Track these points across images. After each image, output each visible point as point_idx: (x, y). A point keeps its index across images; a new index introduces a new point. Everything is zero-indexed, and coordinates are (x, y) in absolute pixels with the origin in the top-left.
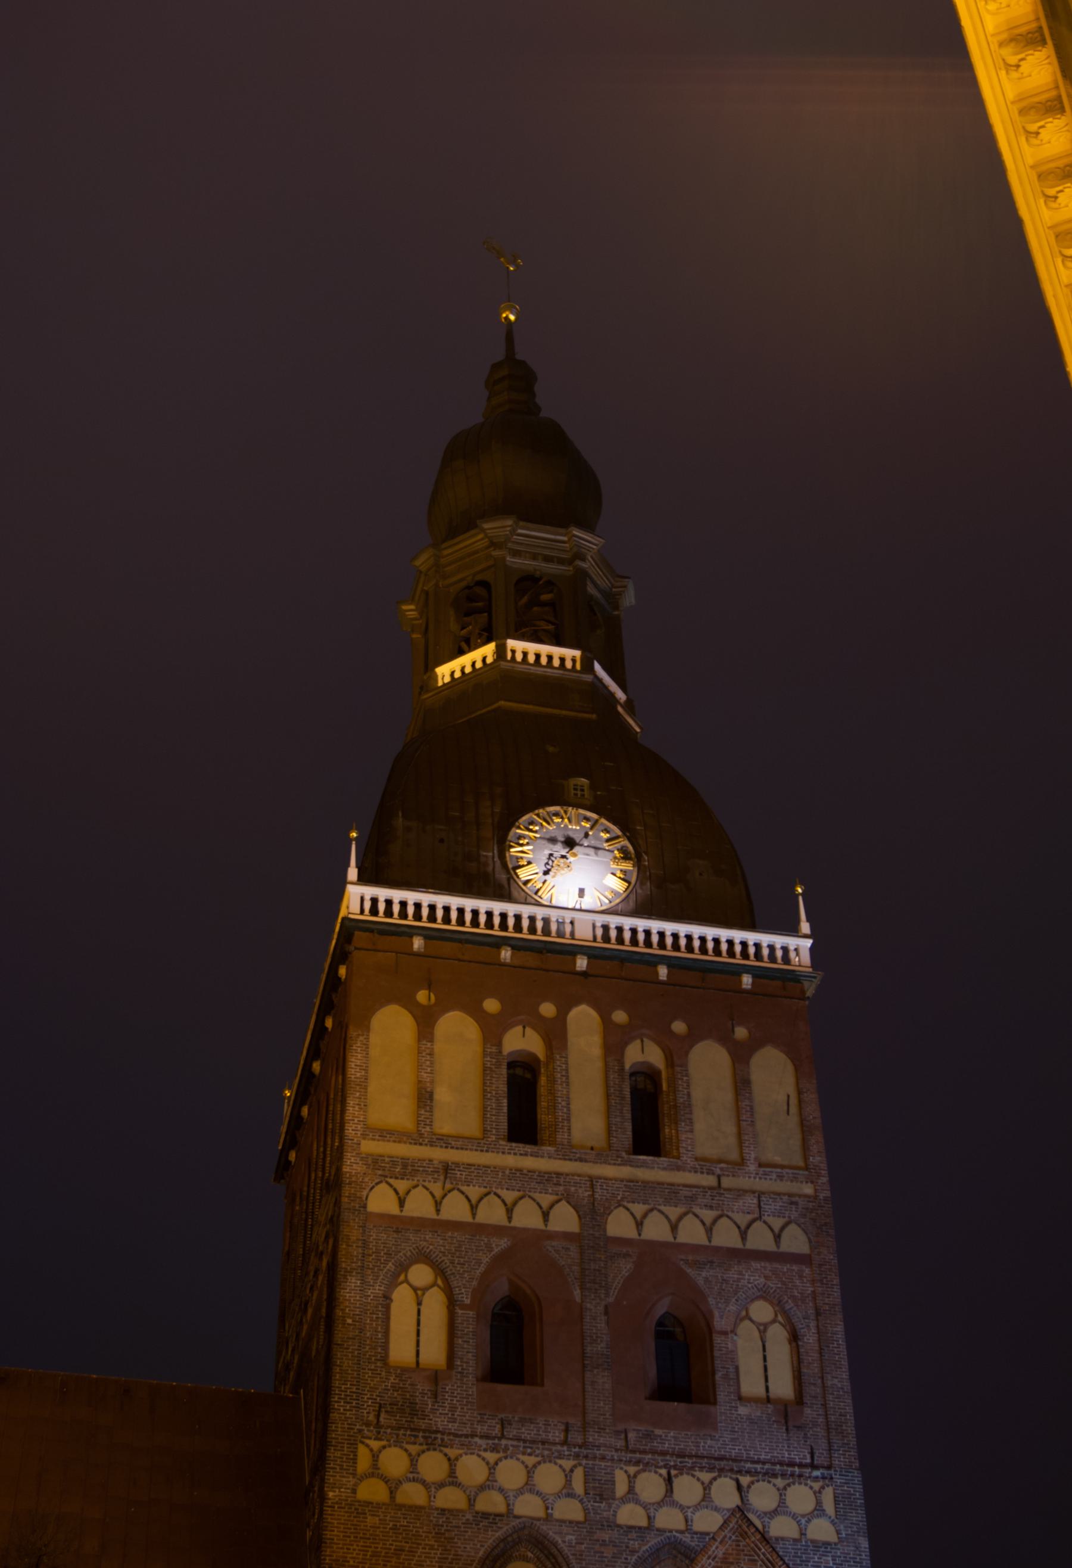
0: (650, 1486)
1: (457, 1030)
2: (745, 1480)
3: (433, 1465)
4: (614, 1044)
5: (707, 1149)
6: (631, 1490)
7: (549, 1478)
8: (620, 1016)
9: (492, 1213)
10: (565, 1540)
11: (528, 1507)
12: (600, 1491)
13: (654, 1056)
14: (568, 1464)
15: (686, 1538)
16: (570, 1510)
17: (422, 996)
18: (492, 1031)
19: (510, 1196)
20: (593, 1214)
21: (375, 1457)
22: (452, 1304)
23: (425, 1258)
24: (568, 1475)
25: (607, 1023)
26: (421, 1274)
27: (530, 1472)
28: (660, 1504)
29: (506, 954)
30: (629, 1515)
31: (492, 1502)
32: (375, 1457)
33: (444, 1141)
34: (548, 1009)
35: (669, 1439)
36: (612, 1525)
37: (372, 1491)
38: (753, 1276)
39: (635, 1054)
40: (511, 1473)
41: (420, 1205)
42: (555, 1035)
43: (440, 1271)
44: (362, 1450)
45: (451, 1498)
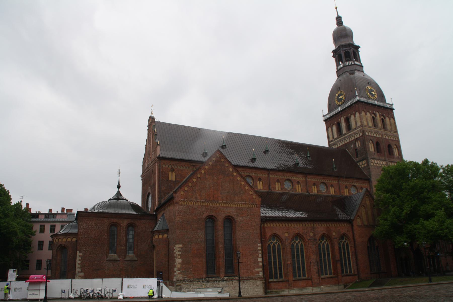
0: (391, 164)
1: (368, 114)
7: (384, 163)
9: (375, 135)
12: (387, 164)
13: (382, 117)
18: (371, 114)
20: (382, 136)
22: (374, 145)
23: (371, 140)
25: (379, 114)
26: (371, 142)
31: (380, 165)
33: (369, 127)
37: (372, 164)
40: (381, 162)
41: (370, 134)
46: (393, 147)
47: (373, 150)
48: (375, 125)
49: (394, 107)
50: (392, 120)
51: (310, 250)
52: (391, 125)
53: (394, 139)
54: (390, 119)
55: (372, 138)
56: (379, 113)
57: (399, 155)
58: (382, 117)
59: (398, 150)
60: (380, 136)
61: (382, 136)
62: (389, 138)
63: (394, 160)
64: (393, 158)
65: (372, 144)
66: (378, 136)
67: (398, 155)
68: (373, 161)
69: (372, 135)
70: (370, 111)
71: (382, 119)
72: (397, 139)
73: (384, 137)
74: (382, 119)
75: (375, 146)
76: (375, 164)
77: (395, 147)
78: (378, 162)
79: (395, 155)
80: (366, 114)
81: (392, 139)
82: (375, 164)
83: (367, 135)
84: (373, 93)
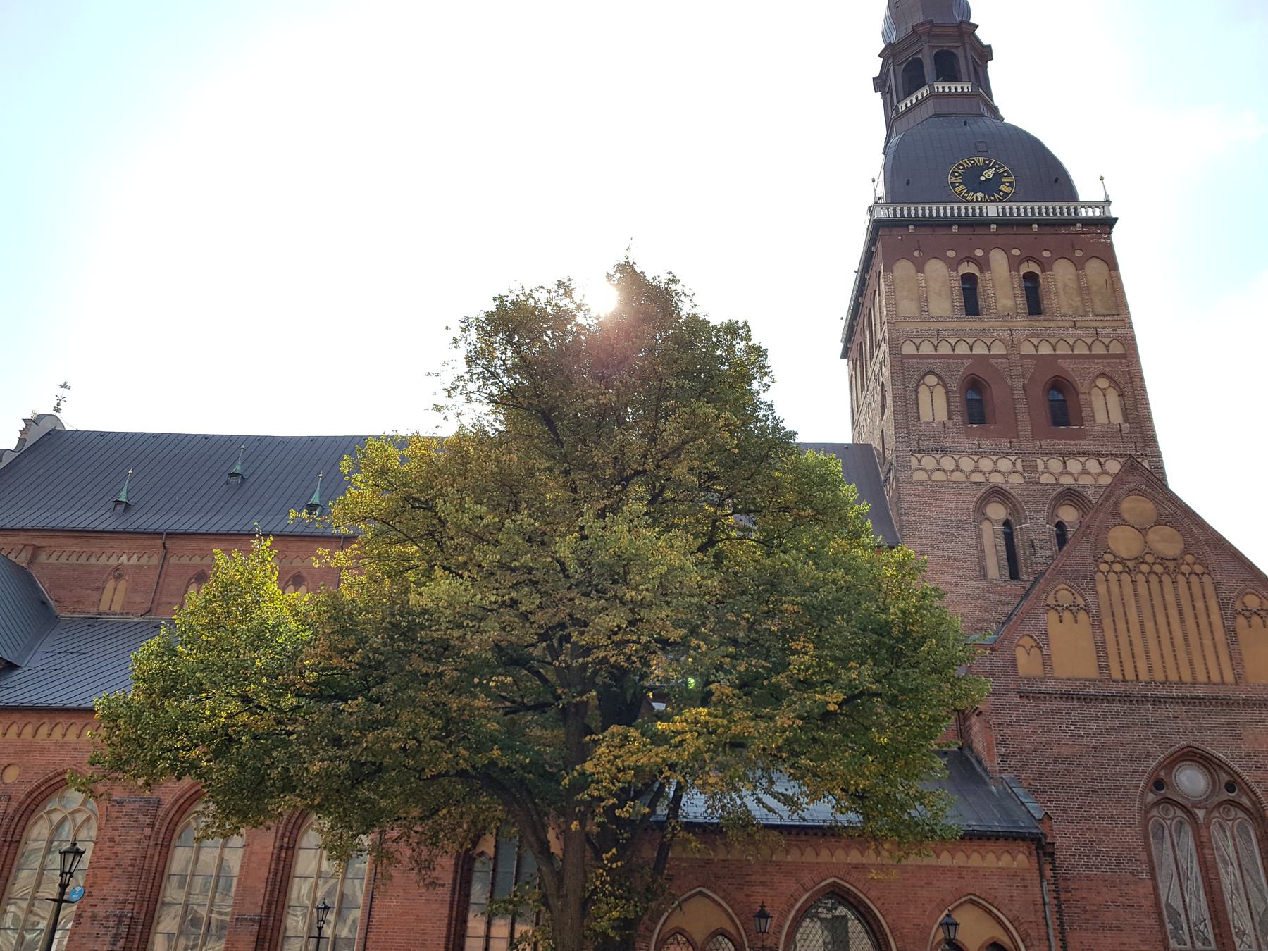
0: (1055, 465)
1: (936, 268)
2: (1102, 460)
3: (948, 463)
4: (1014, 264)
5: (1065, 310)
6: (1045, 467)
7: (1005, 465)
8: (1016, 252)
9: (962, 349)
10: (1016, 493)
11: (997, 479)
13: (1033, 267)
14: (1013, 458)
15: (1076, 487)
16: (1016, 479)
17: (916, 254)
18: (953, 265)
19: (970, 341)
21: (919, 461)
22: (947, 392)
24: (1014, 463)
25: (1009, 256)
26: (931, 380)
27: (995, 463)
28: (1061, 474)
29: (955, 228)
30: (1045, 479)
31: (977, 477)
32: (919, 461)
34: (979, 253)
35: (1061, 445)
36: (1038, 483)
37: (920, 476)
38: (1099, 367)
39: (1025, 269)
40: (986, 464)
41: (927, 349)
42: (984, 264)
43: (939, 377)
44: (913, 459)
45: (957, 476)
46: (1082, 390)
47: (942, 415)
48: (972, 306)
49: (1114, 211)
50: (1095, 268)
51: (107, 853)
52: (1084, 291)
53: (1099, 349)
54: (1079, 265)
55: (936, 365)
56: (1006, 251)
57: (1126, 421)
58: (1033, 267)
59: (1122, 395)
60: (998, 349)
61: (1012, 344)
62: (1063, 349)
63: (1085, 445)
64: (1080, 436)
65: (940, 391)
66: (980, 349)
67: (1117, 418)
68: (928, 462)
69: (944, 349)
70: (951, 254)
71: (1030, 278)
72: (1116, 348)
73: (1027, 349)
74: (1030, 278)
75: (956, 397)
76: (938, 476)
77: (1103, 383)
78: (967, 463)
79: (1101, 418)
80: (920, 269)
81: (1081, 349)
82: (938, 476)
83: (913, 356)
84: (989, 174)
